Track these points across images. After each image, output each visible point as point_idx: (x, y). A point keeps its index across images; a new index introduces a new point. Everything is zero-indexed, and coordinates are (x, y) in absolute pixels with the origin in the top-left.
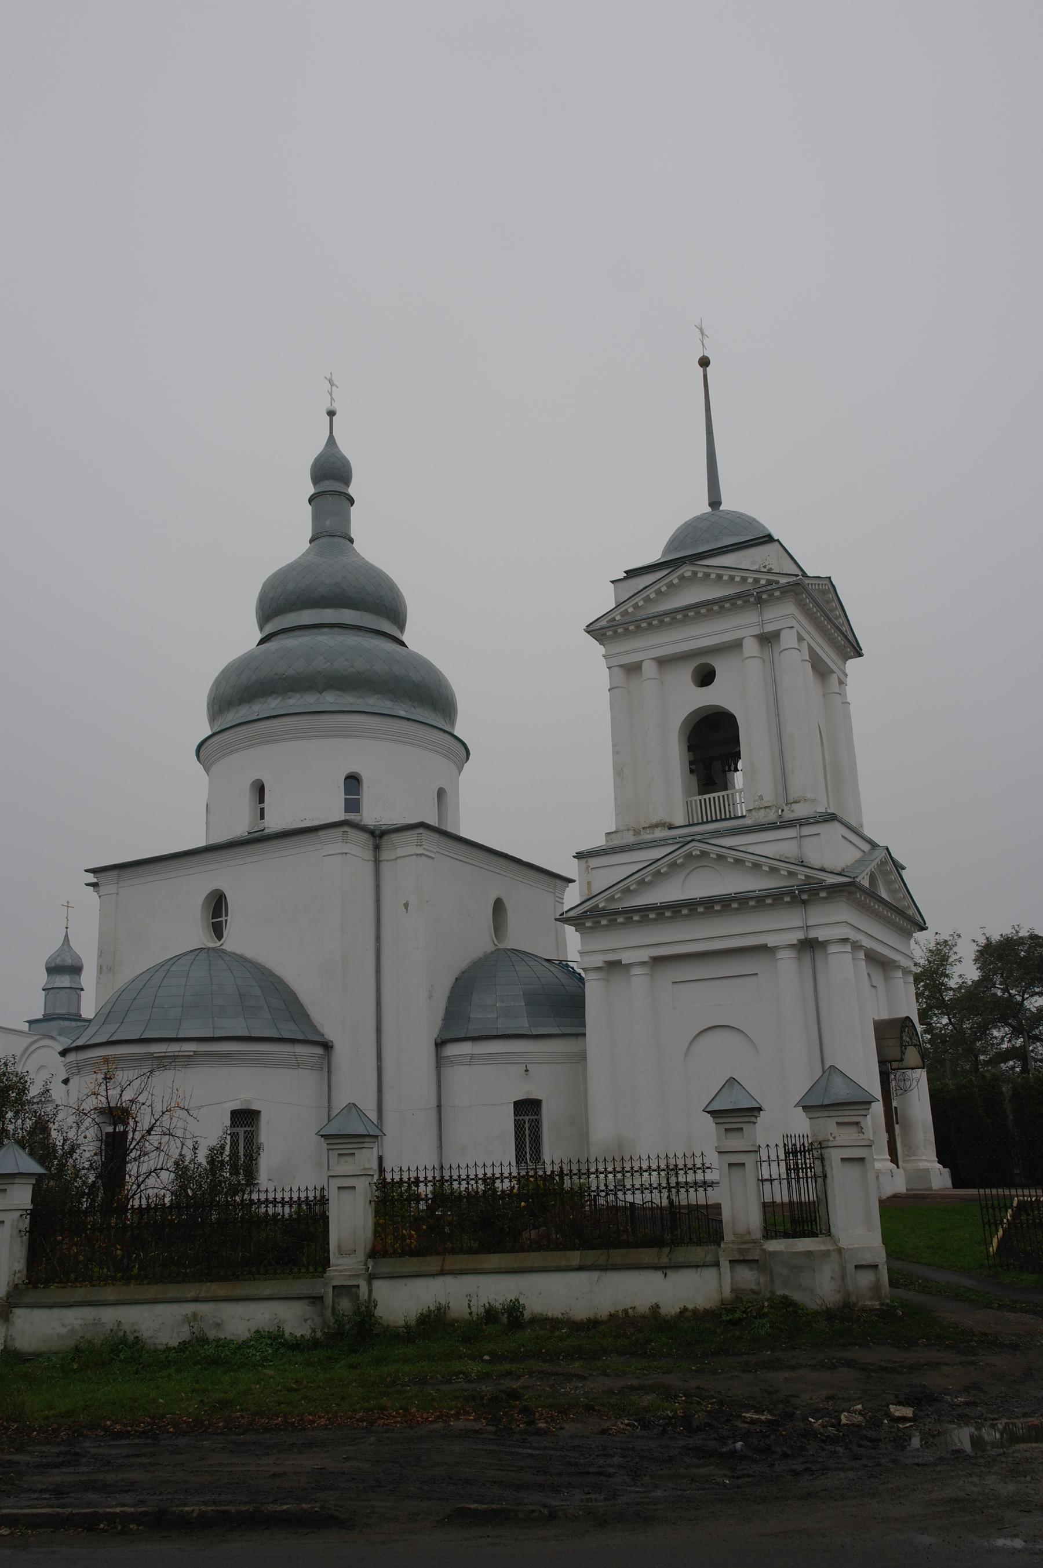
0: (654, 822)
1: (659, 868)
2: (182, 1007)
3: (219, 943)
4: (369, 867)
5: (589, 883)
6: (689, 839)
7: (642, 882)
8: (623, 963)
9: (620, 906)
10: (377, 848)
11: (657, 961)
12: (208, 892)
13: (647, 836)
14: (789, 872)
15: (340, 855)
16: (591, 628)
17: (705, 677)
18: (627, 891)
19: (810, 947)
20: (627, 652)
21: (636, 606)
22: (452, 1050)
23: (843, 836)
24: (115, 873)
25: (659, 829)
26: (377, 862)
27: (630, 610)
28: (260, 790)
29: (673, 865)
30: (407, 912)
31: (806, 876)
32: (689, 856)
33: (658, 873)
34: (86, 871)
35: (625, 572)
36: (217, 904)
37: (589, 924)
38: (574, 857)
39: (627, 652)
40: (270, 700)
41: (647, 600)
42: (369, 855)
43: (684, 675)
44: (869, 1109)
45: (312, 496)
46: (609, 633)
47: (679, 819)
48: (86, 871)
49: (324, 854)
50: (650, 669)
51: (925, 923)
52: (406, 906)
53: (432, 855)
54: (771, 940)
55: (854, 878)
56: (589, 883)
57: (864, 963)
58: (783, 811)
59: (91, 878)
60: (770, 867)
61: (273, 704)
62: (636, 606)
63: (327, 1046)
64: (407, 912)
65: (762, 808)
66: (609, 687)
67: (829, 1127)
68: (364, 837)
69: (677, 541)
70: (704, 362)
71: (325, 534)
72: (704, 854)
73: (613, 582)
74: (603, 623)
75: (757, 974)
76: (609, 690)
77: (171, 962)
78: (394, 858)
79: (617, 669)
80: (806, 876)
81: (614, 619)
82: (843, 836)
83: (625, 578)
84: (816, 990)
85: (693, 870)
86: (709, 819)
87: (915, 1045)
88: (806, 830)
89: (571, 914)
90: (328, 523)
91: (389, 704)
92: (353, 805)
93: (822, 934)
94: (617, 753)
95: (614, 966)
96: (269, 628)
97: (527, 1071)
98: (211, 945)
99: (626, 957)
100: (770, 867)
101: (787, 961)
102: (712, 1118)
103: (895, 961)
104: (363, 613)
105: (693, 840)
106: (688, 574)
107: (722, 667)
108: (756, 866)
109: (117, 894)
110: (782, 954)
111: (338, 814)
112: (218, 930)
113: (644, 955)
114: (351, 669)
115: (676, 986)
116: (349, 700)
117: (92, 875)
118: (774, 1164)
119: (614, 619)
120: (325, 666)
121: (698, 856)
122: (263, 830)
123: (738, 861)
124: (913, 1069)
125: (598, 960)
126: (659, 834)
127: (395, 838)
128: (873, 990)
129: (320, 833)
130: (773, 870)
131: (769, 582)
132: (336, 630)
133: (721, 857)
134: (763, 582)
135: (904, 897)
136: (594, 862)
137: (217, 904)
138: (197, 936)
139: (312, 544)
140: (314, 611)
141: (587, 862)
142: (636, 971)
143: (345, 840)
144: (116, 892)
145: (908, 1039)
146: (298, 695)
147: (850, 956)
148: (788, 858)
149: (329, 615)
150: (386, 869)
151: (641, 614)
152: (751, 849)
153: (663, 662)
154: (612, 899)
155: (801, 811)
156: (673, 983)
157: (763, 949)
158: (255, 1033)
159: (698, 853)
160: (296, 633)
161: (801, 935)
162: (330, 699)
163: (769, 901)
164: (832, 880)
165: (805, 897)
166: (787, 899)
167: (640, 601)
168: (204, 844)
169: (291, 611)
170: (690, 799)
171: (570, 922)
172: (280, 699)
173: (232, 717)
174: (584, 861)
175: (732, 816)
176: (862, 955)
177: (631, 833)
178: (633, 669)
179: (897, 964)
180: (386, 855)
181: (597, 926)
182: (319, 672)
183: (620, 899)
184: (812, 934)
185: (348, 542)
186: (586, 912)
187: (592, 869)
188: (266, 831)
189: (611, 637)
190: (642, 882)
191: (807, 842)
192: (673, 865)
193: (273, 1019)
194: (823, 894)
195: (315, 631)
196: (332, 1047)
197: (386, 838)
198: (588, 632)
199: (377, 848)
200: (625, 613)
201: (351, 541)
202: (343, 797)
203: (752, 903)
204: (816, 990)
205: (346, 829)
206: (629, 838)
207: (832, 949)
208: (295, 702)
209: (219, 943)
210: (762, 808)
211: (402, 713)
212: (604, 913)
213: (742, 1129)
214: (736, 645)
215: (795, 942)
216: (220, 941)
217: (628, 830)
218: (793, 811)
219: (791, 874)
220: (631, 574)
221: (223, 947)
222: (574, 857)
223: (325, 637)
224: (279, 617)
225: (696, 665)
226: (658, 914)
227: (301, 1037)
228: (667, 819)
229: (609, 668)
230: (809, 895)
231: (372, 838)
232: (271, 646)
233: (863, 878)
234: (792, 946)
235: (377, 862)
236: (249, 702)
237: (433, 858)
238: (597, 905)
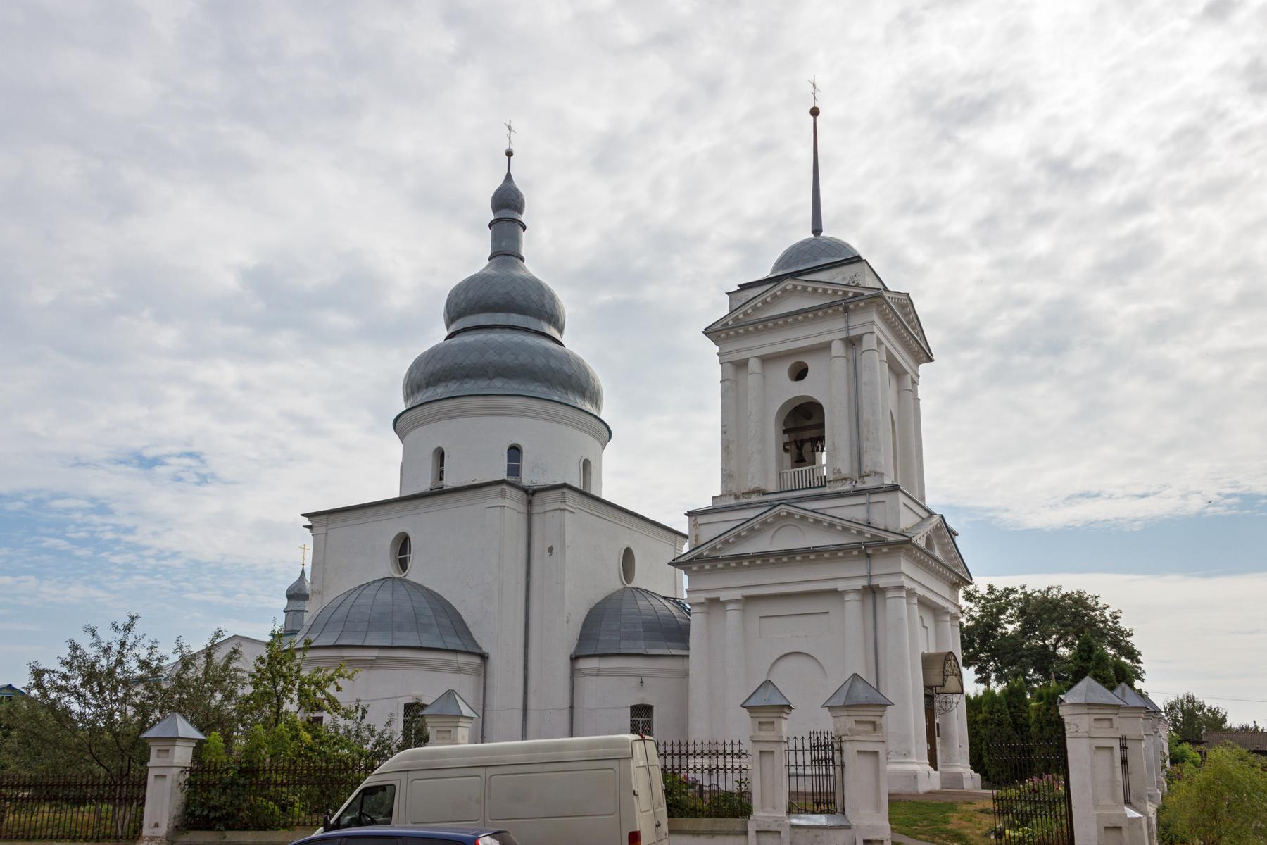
0: (752, 489)
2: (369, 622)
3: (404, 575)
4: (522, 519)
5: (697, 536)
6: (777, 503)
7: (738, 536)
8: (721, 599)
9: (720, 554)
10: (530, 503)
11: (748, 599)
12: (397, 533)
13: (745, 501)
14: (857, 531)
15: (499, 508)
16: (708, 331)
17: (800, 373)
18: (726, 542)
19: (872, 592)
20: (736, 351)
21: (745, 314)
23: (904, 504)
24: (324, 517)
25: (756, 494)
26: (529, 515)
27: (741, 316)
28: (440, 455)
29: (765, 523)
30: (550, 555)
31: (871, 535)
32: (778, 516)
33: (752, 529)
34: (303, 515)
35: (739, 286)
36: (403, 545)
37: (695, 568)
38: (686, 514)
39: (736, 351)
40: (450, 384)
42: (523, 509)
43: (782, 371)
44: (884, 711)
45: (491, 222)
46: (723, 335)
47: (772, 487)
48: (303, 515)
49: (487, 506)
50: (754, 365)
51: (972, 579)
52: (550, 550)
53: (574, 510)
54: (841, 586)
55: (911, 538)
56: (697, 536)
57: (916, 607)
58: (856, 482)
59: (307, 522)
60: (842, 527)
61: (453, 388)
62: (745, 314)
64: (550, 555)
65: (839, 480)
66: (720, 379)
67: (846, 723)
68: (518, 494)
71: (500, 253)
72: (790, 515)
73: (728, 293)
74: (718, 326)
75: (828, 612)
76: (721, 382)
77: (365, 586)
78: (543, 511)
79: (728, 365)
80: (871, 535)
81: (727, 324)
82: (904, 504)
83: (738, 290)
84: (875, 628)
85: (780, 528)
86: (801, 487)
87: (956, 675)
88: (874, 498)
89: (681, 560)
90: (504, 244)
91: (545, 390)
92: (514, 470)
93: (881, 582)
94: (725, 433)
95: (714, 602)
96: (453, 328)
98: (397, 576)
99: (724, 596)
100: (842, 527)
101: (852, 603)
102: (748, 713)
103: (944, 608)
104: (529, 318)
105: (781, 504)
107: (813, 364)
108: (832, 525)
109: (326, 534)
110: (848, 597)
111: (502, 475)
112: (403, 564)
113: (738, 594)
114: (516, 362)
115: (763, 620)
116: (513, 386)
117: (307, 518)
118: (799, 753)
119: (727, 324)
120: (495, 358)
121: (784, 516)
122: (442, 488)
123: (817, 522)
124: (953, 694)
125: (701, 597)
126: (754, 498)
127: (544, 495)
128: (925, 629)
129: (486, 490)
130: (845, 529)
132: (507, 330)
133: (803, 518)
135: (955, 557)
136: (701, 519)
137: (403, 545)
138: (387, 568)
139: (491, 261)
140: (489, 314)
141: (696, 519)
142: (730, 607)
143: (503, 497)
144: (325, 532)
145: (950, 670)
146: (473, 381)
147: (905, 600)
148: (858, 520)
149: (501, 318)
150: (536, 520)
151: (749, 319)
152: (828, 512)
153: (765, 360)
155: (870, 483)
156: (761, 617)
157: (834, 592)
158: (425, 645)
159: (785, 514)
160: (474, 332)
161: (865, 582)
162: (498, 385)
163: (840, 554)
164: (892, 538)
165: (870, 551)
166: (855, 553)
167: (749, 309)
168: (398, 496)
169: (470, 314)
170: (782, 472)
172: (458, 383)
173: (421, 397)
174: (694, 518)
175: (816, 485)
176: (915, 600)
177: (732, 497)
178: (741, 365)
179: (946, 610)
180: (537, 509)
181: (701, 569)
182: (490, 363)
184: (875, 582)
185: (520, 261)
186: (693, 559)
187: (700, 525)
188: (445, 488)
189: (724, 339)
190: (738, 536)
191: (875, 508)
192: (765, 523)
193: (441, 634)
194: (885, 550)
195: (490, 330)
197: (537, 495)
198: (706, 334)
199: (530, 503)
200: (736, 319)
201: (522, 259)
202: (506, 463)
203: (826, 555)
204: (875, 628)
205: (504, 487)
206: (732, 502)
207: (890, 594)
208: (470, 386)
209: (404, 575)
210: (839, 480)
211: (556, 398)
212: (707, 559)
213: (773, 723)
215: (860, 588)
216: (404, 572)
217: (731, 495)
218: (864, 483)
219: (860, 533)
220: (744, 287)
221: (407, 578)
222: (686, 514)
223: (496, 335)
224: (462, 319)
225: (790, 365)
226: (750, 562)
227: (462, 648)
228: (763, 487)
229: (721, 364)
230: (873, 550)
231: (525, 495)
232: (455, 340)
233: (920, 539)
234: (857, 591)
236: (434, 386)
237: (574, 513)
238: (702, 554)
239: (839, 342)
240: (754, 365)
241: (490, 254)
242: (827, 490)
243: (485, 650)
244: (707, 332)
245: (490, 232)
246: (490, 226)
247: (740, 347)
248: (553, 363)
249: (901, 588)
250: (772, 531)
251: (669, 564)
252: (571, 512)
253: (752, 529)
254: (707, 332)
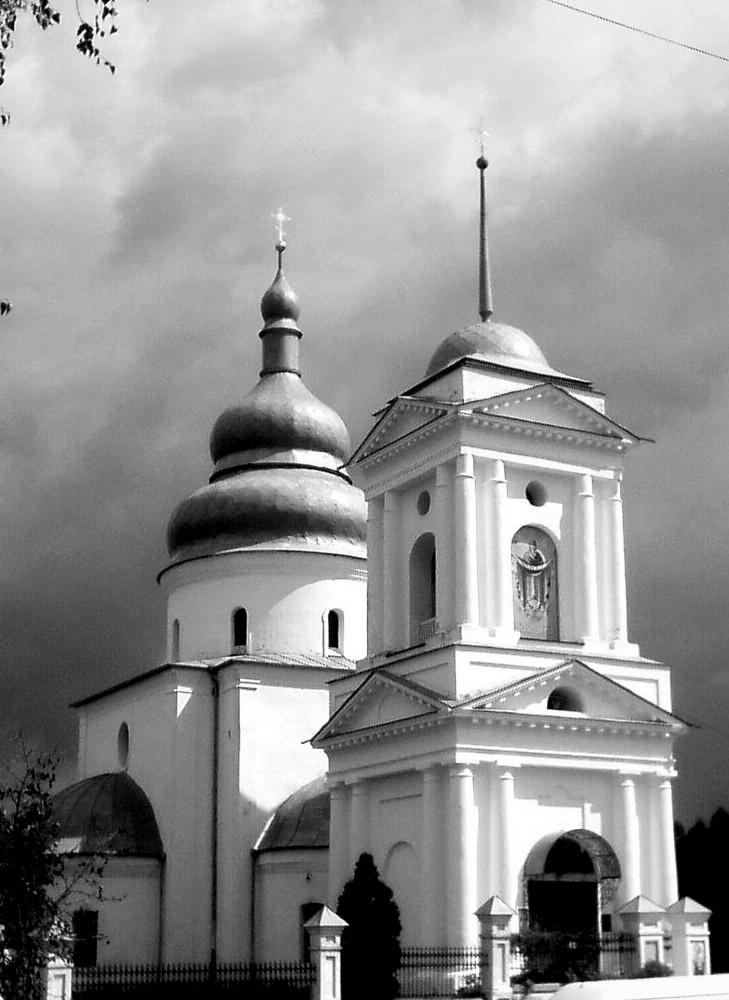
17: (424, 504)
22: (266, 860)
26: (215, 692)
41: (382, 435)
42: (208, 687)
50: (389, 501)
54: (421, 764)
63: (161, 858)
69: (434, 363)
93: (444, 760)
97: (308, 878)
106: (402, 408)
110: (427, 777)
134: (440, 413)
153: (401, 492)
157: (413, 774)
196: (165, 859)
205: (173, 671)
214: (430, 477)
235: (215, 692)
237: (255, 689)
238: (330, 732)
240: (389, 501)
241: (261, 369)
242: (427, 649)
243: (167, 849)
245: (260, 341)
246: (262, 335)
248: (280, 504)
249: (461, 766)
250: (380, 701)
252: (250, 689)
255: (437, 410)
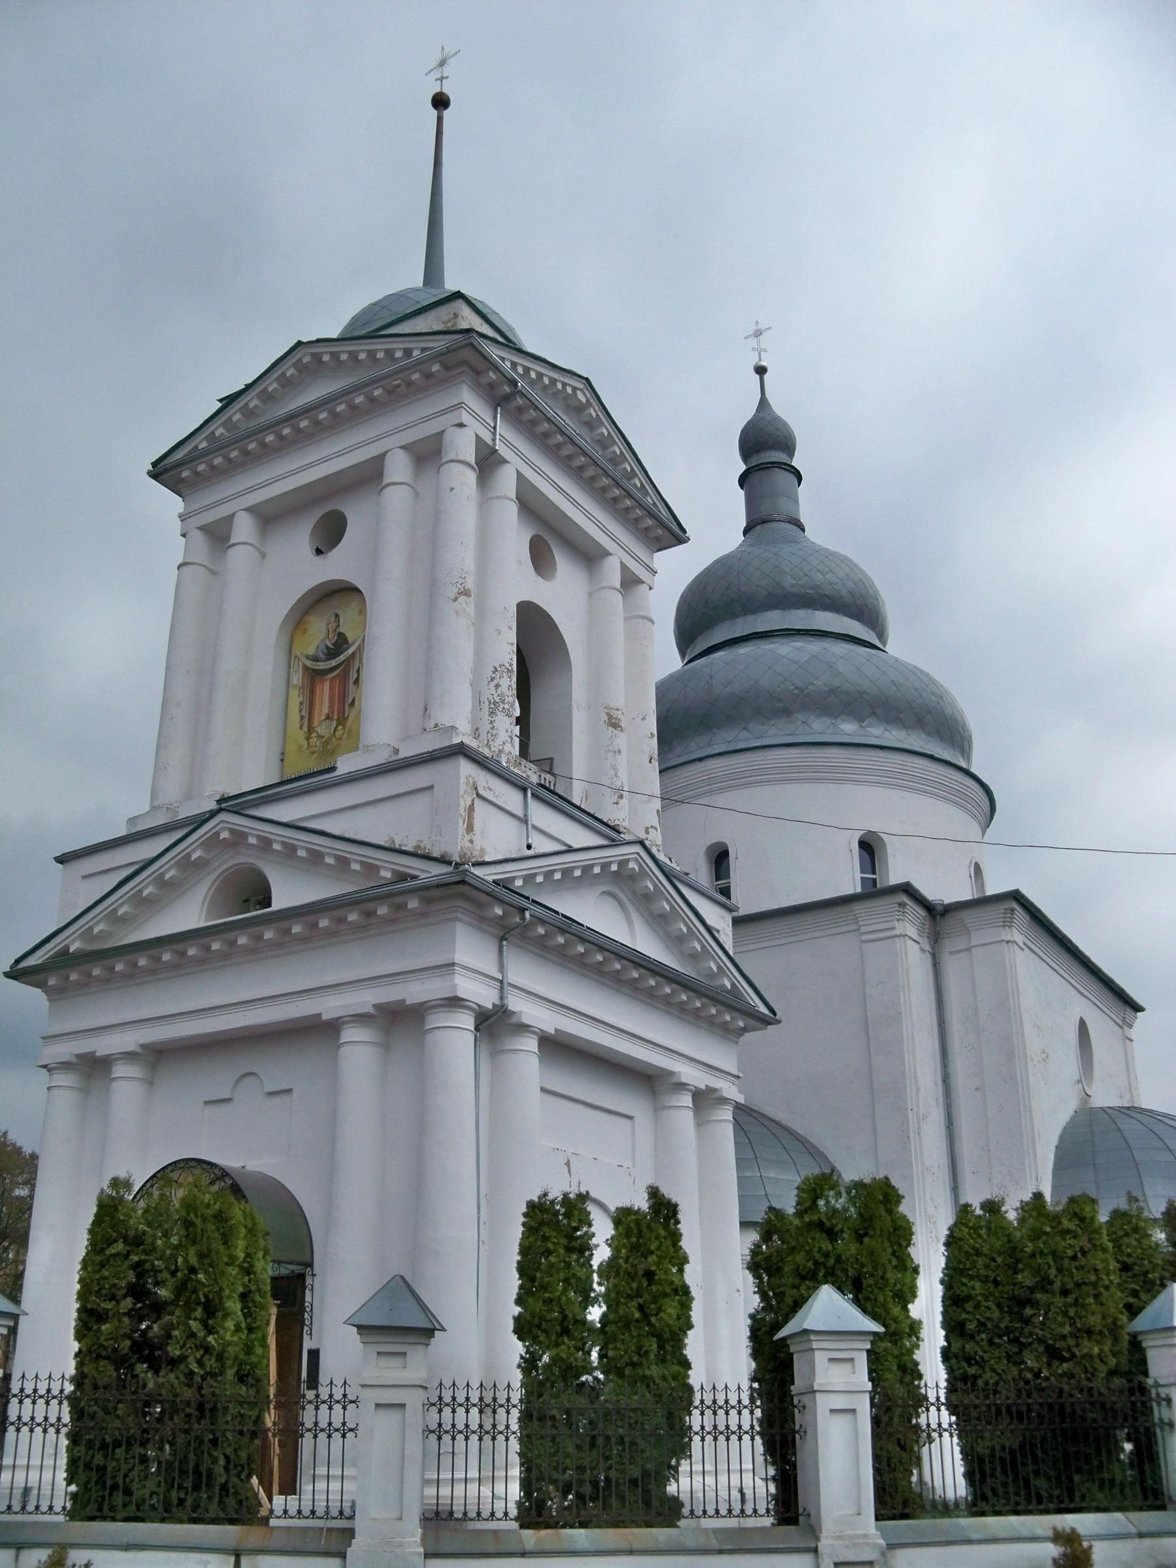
1: (161, 871)
54: (330, 1007)
57: (534, 1061)
70: (440, 102)
93: (416, 992)
99: (103, 1046)
108: (316, 857)
131: (423, 350)
154: (88, 934)
171: (24, 980)
183: (101, 936)
238: (67, 947)
239: (401, 452)
244: (161, 471)
247: (217, 497)
251: (7, 975)
253: (162, 883)
254: (161, 471)
255: (408, 352)
